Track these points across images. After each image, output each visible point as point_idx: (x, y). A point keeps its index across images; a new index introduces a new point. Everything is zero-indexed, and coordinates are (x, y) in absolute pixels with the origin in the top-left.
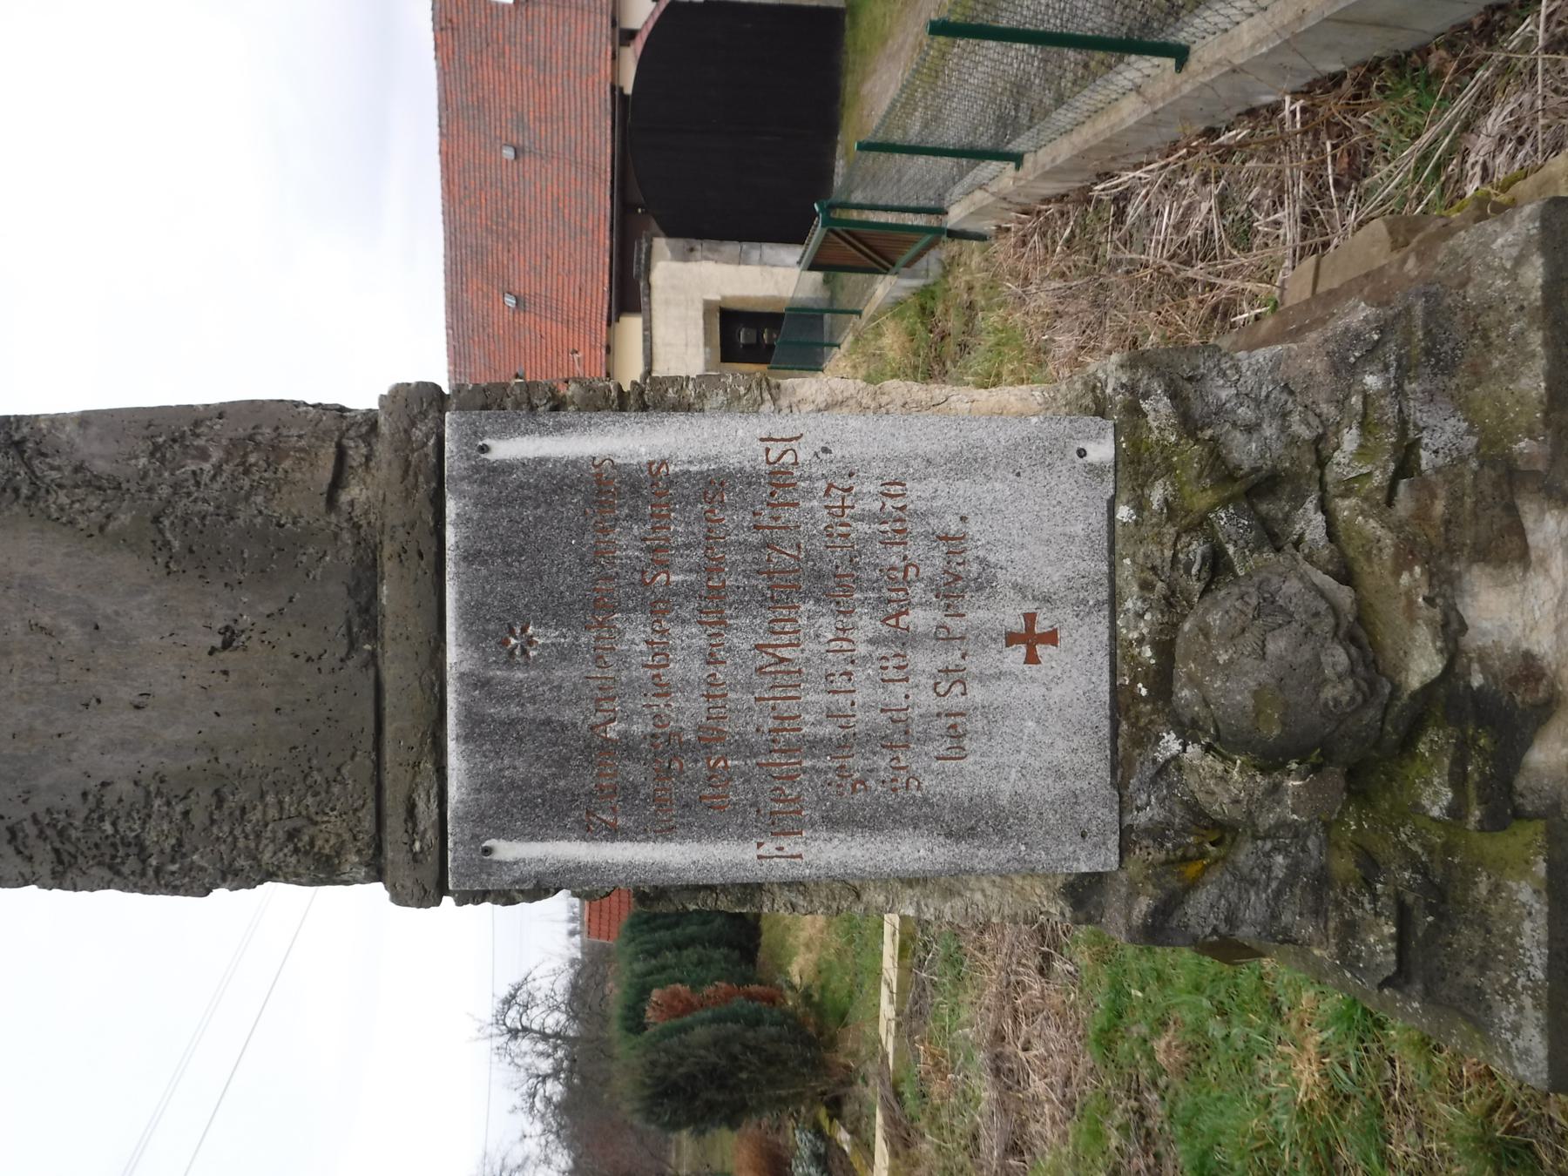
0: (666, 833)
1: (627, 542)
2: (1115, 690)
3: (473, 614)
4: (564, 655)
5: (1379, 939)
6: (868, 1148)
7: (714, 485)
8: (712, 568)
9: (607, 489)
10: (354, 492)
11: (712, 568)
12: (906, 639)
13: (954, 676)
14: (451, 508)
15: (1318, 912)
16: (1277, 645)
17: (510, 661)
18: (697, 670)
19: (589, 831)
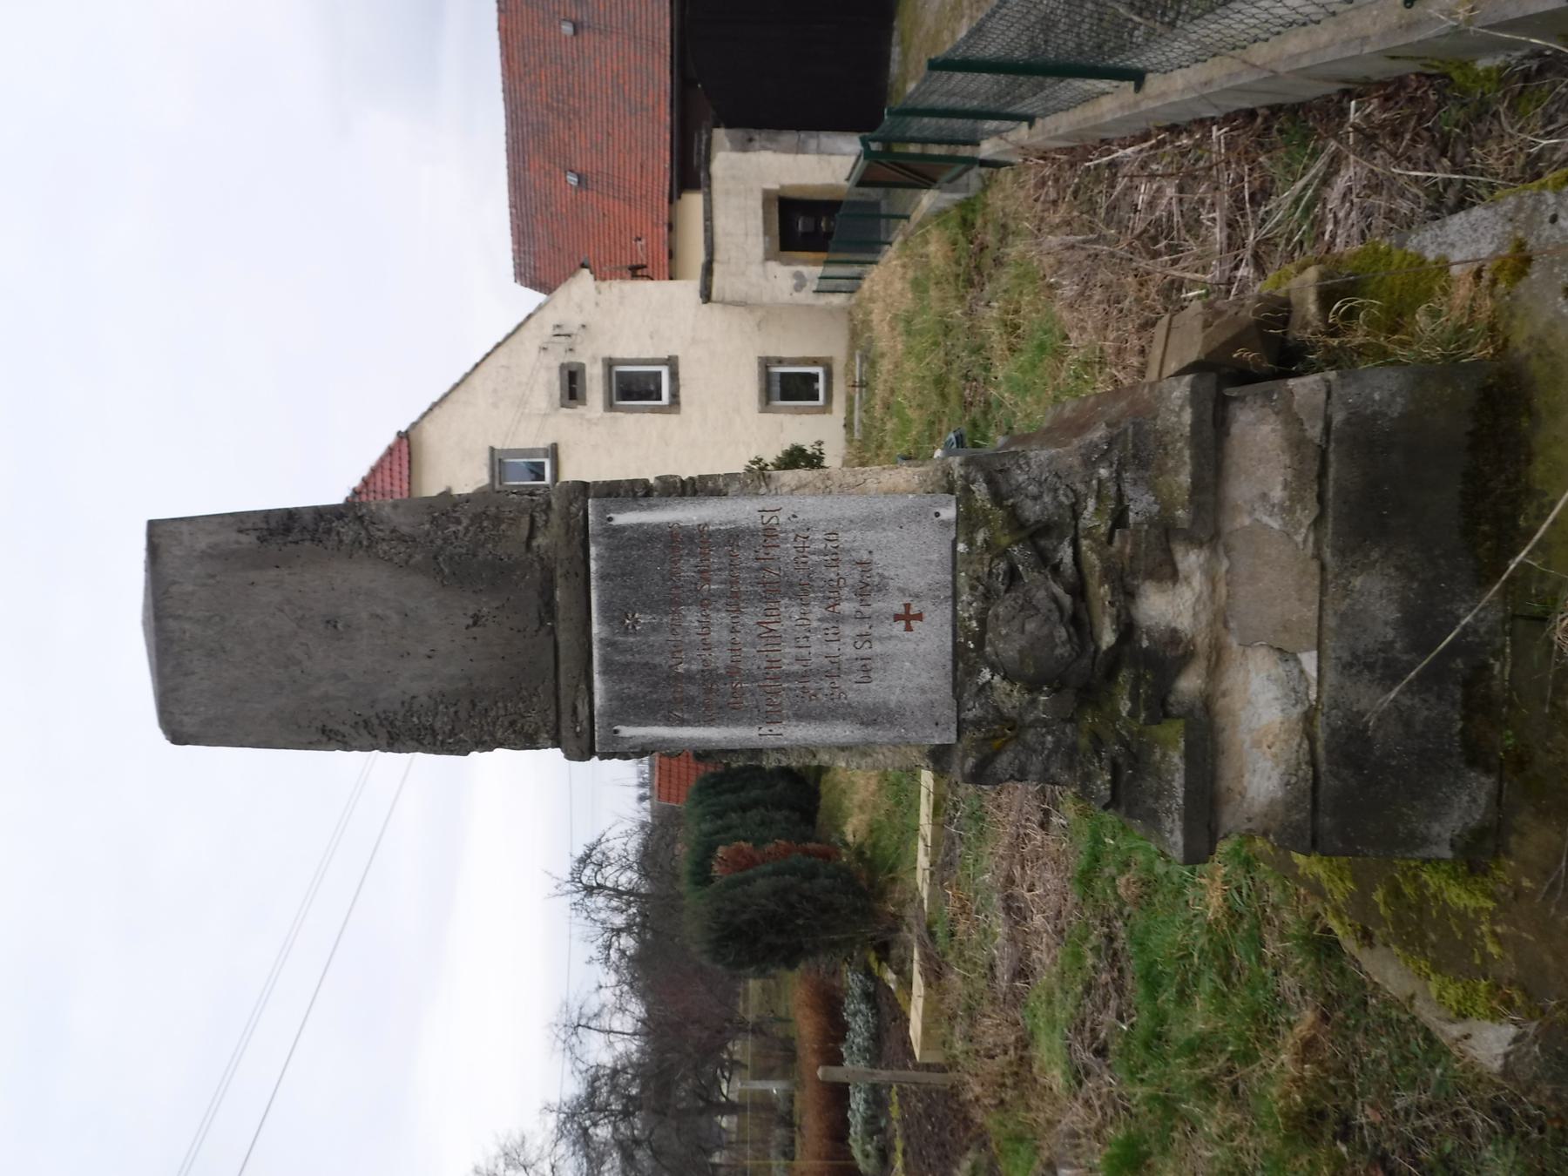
0: (709, 722)
1: (687, 568)
2: (955, 645)
3: (605, 608)
4: (655, 629)
6: (907, 984)
7: (733, 537)
9: (676, 540)
10: (540, 541)
12: (839, 619)
13: (865, 638)
14: (593, 551)
15: (1070, 767)
16: (1031, 626)
17: (626, 633)
18: (726, 636)
19: (669, 721)
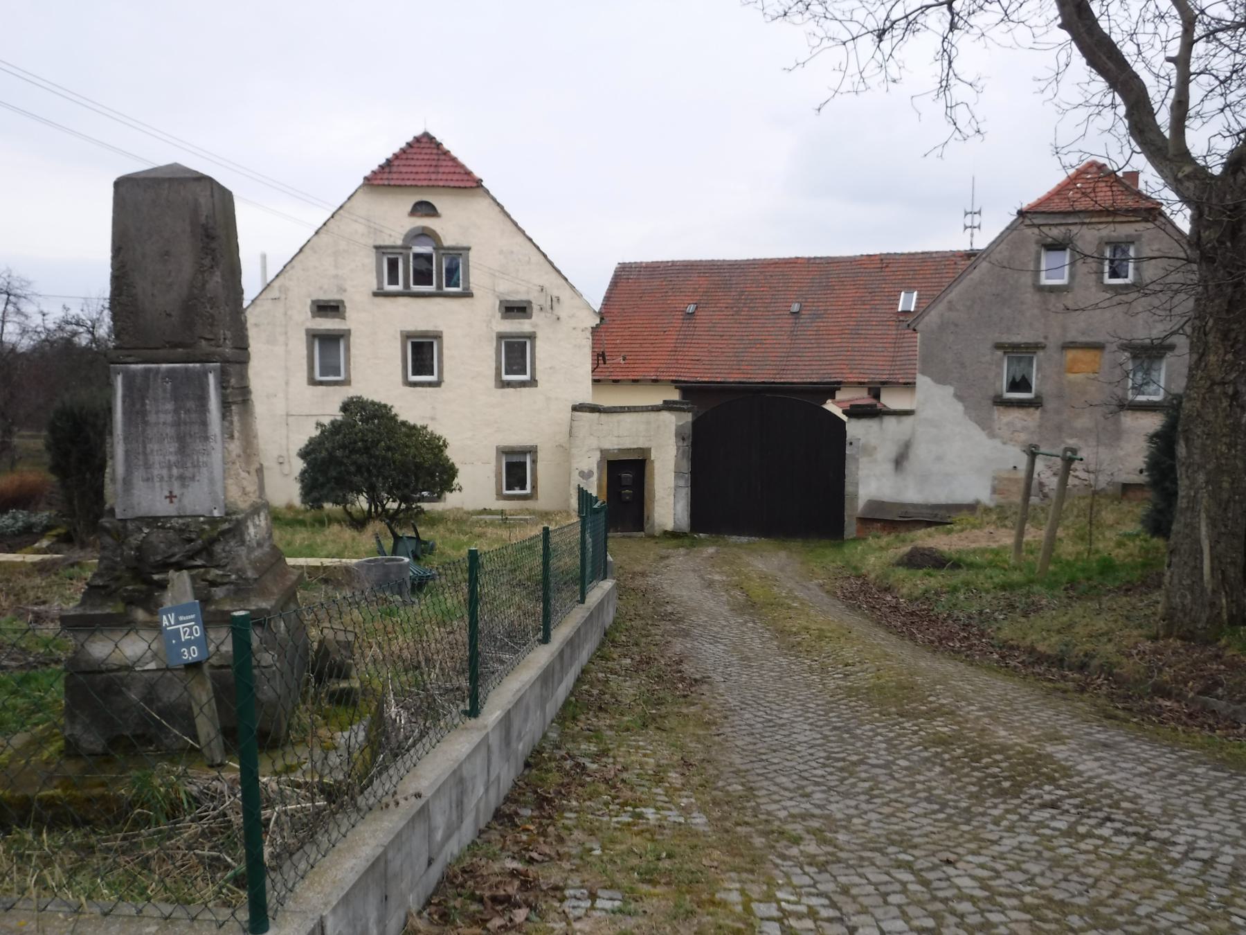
0: (124, 413)
1: (191, 404)
2: (159, 518)
3: (173, 370)
4: (165, 391)
5: (99, 582)
6: (38, 552)
7: (204, 424)
8: (185, 424)
9: (203, 400)
10: (203, 342)
11: (185, 424)
12: (170, 468)
13: (162, 479)
14: (198, 365)
15: (106, 568)
16: (162, 545)
17: (163, 378)
18: (162, 420)
19: (124, 396)
